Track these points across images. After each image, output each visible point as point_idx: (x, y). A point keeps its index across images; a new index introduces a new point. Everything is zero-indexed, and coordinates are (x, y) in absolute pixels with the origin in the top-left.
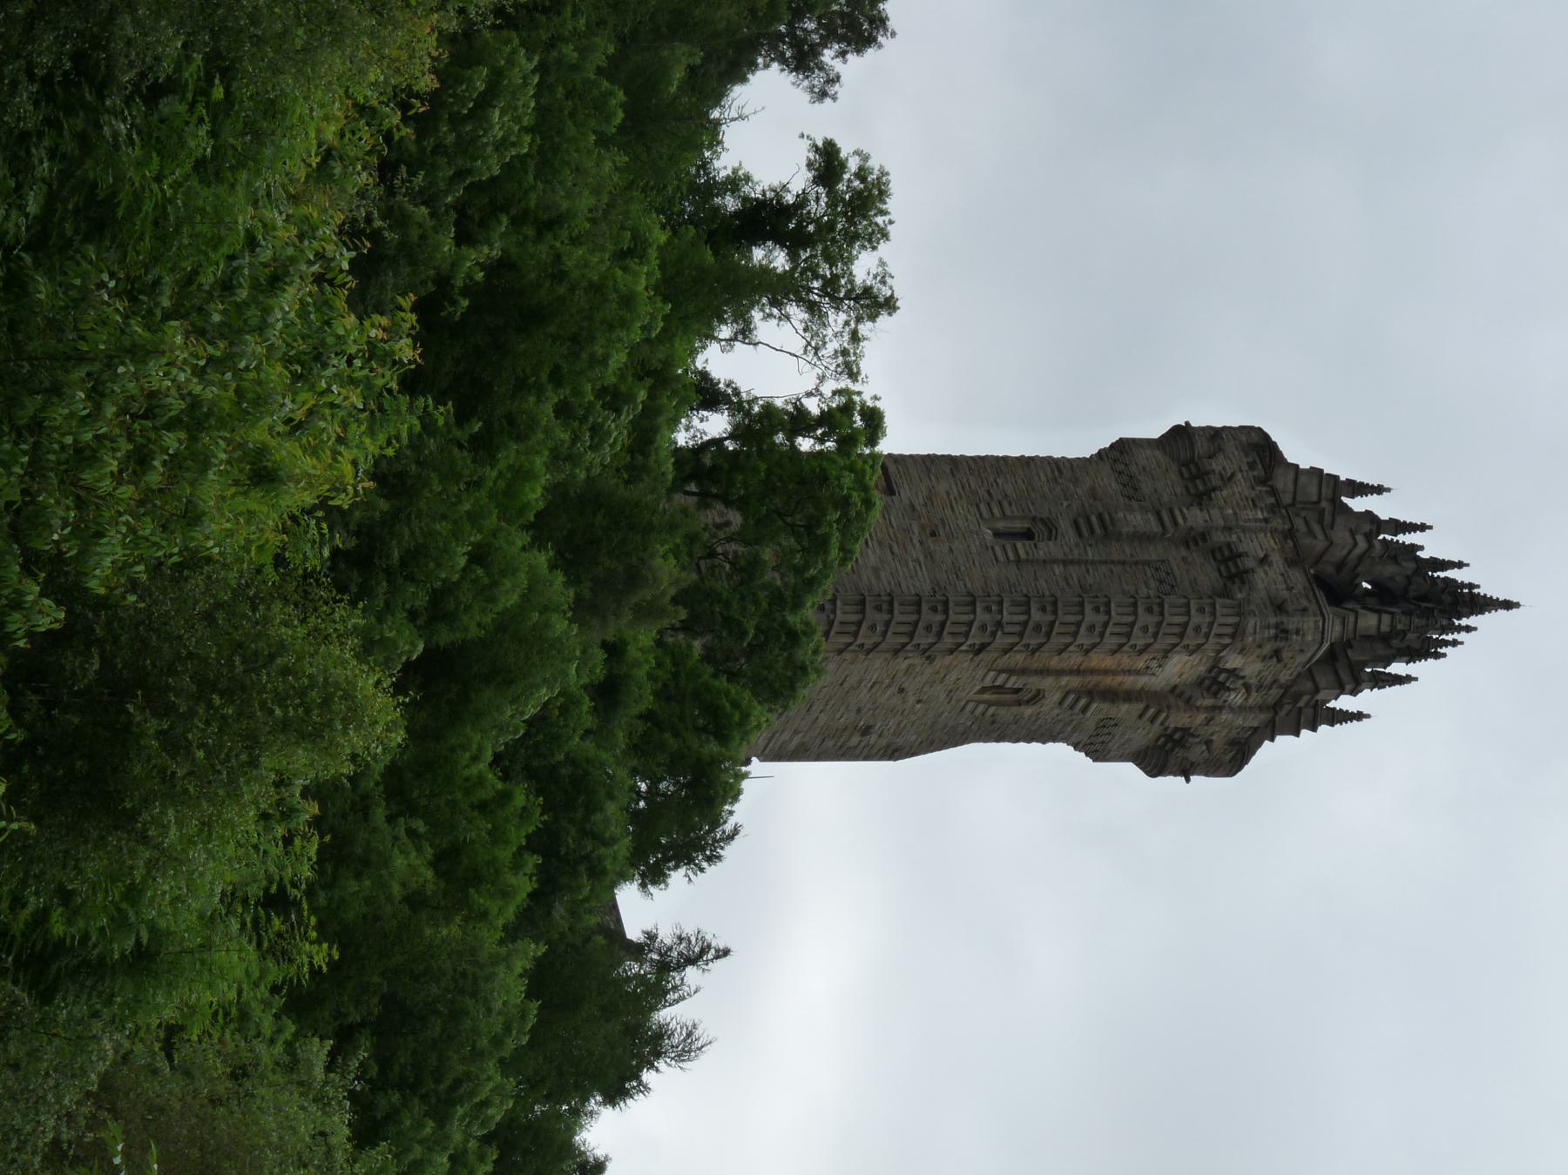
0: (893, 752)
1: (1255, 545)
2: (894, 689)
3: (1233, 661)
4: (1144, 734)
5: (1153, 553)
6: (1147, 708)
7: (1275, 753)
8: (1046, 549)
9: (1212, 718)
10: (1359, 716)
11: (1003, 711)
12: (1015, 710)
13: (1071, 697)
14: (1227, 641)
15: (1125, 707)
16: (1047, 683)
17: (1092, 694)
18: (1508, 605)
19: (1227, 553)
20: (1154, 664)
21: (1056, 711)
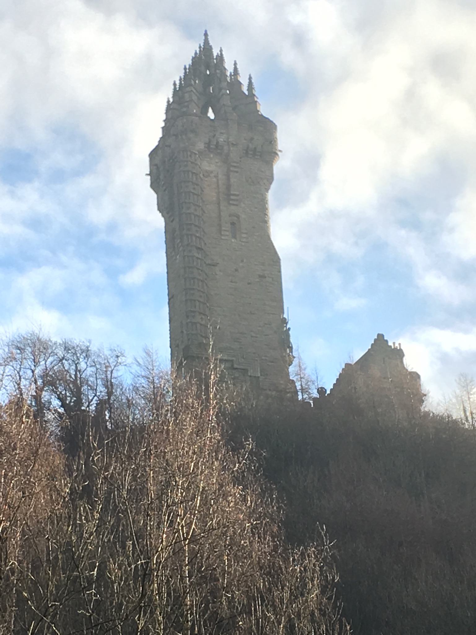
3: (201, 146)
6: (232, 171)
9: (232, 144)
13: (231, 202)
14: (189, 153)
15: (232, 180)
17: (228, 195)
18: (206, 34)
19: (171, 161)
20: (212, 175)
21: (243, 205)
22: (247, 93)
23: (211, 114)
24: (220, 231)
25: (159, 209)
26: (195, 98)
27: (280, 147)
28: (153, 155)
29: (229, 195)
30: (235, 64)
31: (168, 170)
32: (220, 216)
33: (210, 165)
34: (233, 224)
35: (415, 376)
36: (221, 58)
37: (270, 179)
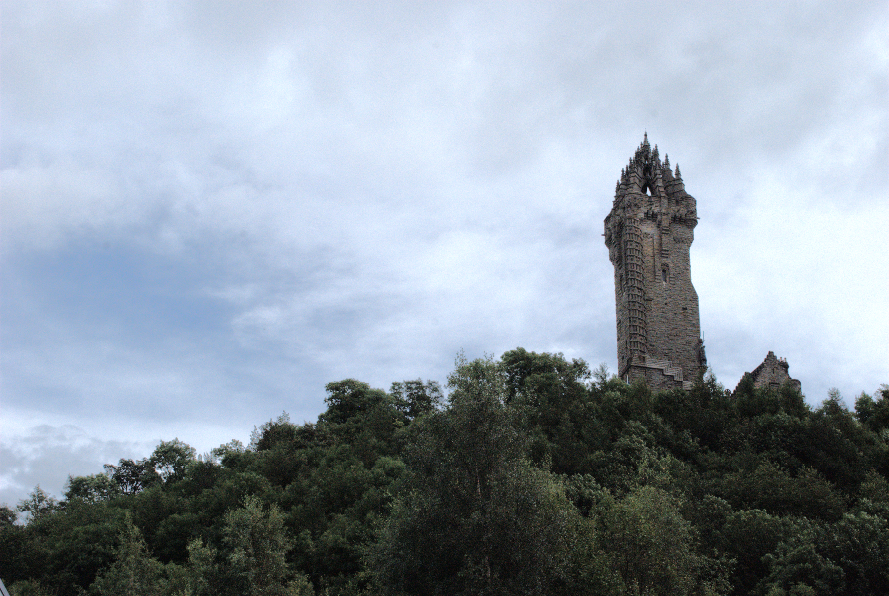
0: (695, 298)
1: (617, 218)
2: (665, 307)
3: (641, 215)
4: (679, 230)
5: (623, 245)
7: (689, 189)
10: (677, 167)
11: (672, 273)
12: (671, 269)
15: (664, 239)
16: (658, 265)
18: (646, 136)
22: (674, 177)
23: (649, 193)
26: (637, 181)
27: (698, 216)
30: (667, 157)
31: (618, 233)
32: (654, 266)
34: (664, 271)
35: (797, 382)
36: (656, 153)
37: (691, 240)
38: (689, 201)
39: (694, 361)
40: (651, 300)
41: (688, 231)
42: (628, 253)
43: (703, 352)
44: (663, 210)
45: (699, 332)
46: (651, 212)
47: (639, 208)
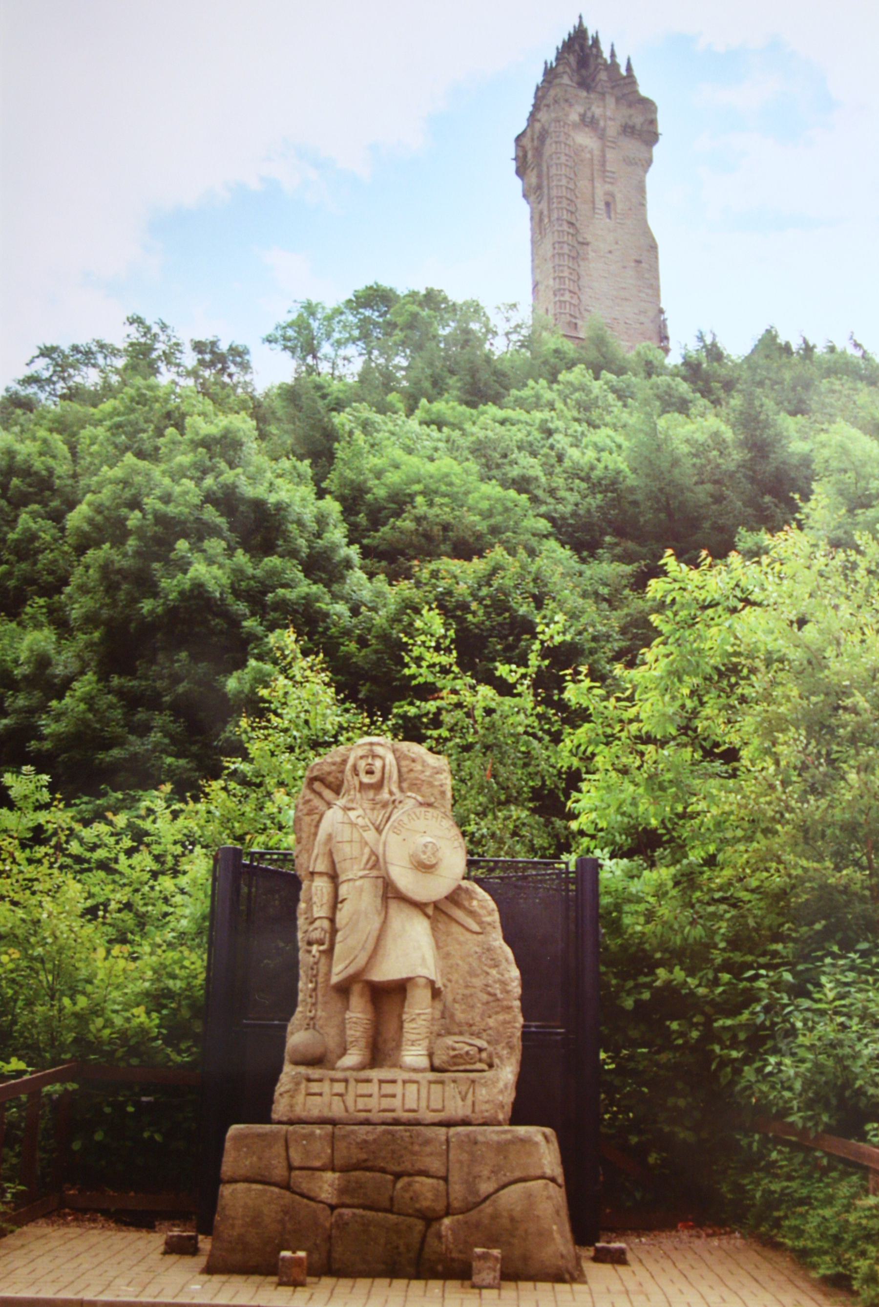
0: (653, 247)
1: (538, 126)
3: (574, 117)
4: (631, 146)
7: (644, 90)
8: (546, 213)
24: (594, 208)
25: (525, 196)
28: (518, 139)
29: (604, 171)
33: (585, 140)
34: (608, 204)
36: (596, 41)
37: (649, 162)
38: (647, 106)
39: (650, 339)
40: (587, 244)
41: (643, 148)
42: (553, 171)
43: (665, 326)
44: (609, 114)
45: (657, 295)
46: (589, 114)
47: (571, 105)
